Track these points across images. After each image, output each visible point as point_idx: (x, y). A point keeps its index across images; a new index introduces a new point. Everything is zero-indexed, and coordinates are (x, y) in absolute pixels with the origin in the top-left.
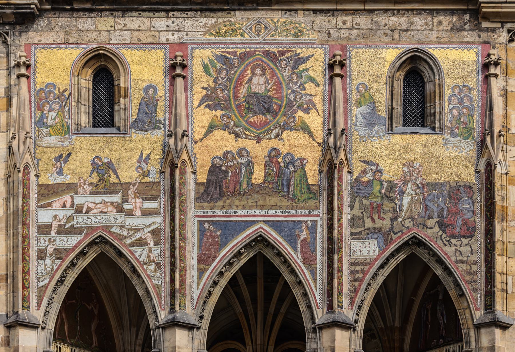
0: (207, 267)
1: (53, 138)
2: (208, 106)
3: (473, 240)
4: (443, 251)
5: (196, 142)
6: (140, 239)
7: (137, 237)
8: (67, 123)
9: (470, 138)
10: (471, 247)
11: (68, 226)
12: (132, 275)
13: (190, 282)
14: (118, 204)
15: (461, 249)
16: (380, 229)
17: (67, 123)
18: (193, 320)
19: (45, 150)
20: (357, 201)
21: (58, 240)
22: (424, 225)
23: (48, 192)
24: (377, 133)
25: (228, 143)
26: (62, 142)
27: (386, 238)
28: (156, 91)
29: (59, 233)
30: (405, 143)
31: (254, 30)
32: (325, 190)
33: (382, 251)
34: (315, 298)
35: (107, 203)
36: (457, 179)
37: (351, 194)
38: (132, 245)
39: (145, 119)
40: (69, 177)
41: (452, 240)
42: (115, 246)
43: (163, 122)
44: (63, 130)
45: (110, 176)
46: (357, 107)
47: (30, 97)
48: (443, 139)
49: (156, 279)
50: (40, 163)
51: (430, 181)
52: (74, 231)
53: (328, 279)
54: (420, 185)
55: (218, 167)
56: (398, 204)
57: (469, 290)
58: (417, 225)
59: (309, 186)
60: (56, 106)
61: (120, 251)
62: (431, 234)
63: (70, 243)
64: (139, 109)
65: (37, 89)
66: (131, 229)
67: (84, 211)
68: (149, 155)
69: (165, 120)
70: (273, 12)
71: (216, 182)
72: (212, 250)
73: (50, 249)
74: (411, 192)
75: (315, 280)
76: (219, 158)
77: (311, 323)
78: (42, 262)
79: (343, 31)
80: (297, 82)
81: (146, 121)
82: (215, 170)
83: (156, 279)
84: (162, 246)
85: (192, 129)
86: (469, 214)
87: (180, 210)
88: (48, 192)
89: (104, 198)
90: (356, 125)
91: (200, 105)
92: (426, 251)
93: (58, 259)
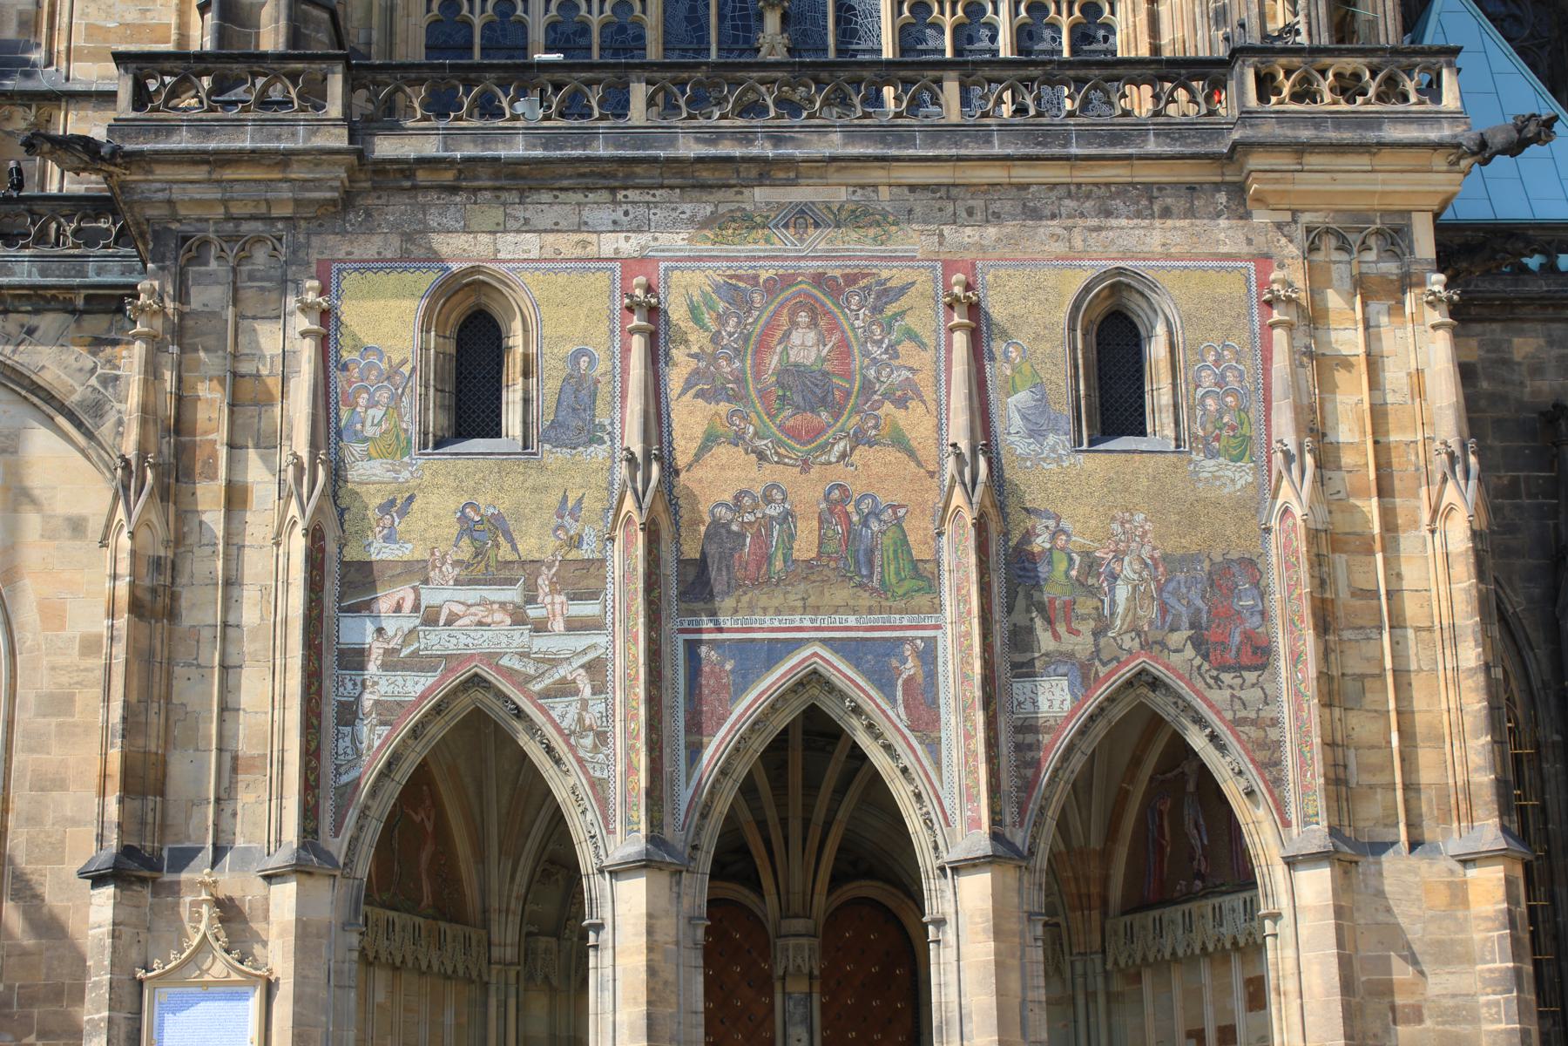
1: (376, 463)
2: (700, 394)
6: (563, 681)
7: (557, 677)
15: (1242, 694)
20: (1021, 595)
21: (383, 682)
22: (1163, 644)
24: (1053, 449)
25: (743, 475)
26: (395, 471)
27: (1084, 676)
35: (492, 603)
38: (546, 694)
39: (575, 423)
40: (410, 546)
41: (1223, 676)
43: (609, 428)
44: (395, 447)
45: (498, 547)
51: (1169, 551)
52: (419, 663)
57: (1265, 782)
59: (915, 564)
60: (383, 396)
61: (517, 707)
62: (1178, 662)
63: (410, 689)
66: (543, 661)
69: (612, 424)
75: (938, 764)
84: (610, 695)
91: (684, 392)
93: (383, 723)
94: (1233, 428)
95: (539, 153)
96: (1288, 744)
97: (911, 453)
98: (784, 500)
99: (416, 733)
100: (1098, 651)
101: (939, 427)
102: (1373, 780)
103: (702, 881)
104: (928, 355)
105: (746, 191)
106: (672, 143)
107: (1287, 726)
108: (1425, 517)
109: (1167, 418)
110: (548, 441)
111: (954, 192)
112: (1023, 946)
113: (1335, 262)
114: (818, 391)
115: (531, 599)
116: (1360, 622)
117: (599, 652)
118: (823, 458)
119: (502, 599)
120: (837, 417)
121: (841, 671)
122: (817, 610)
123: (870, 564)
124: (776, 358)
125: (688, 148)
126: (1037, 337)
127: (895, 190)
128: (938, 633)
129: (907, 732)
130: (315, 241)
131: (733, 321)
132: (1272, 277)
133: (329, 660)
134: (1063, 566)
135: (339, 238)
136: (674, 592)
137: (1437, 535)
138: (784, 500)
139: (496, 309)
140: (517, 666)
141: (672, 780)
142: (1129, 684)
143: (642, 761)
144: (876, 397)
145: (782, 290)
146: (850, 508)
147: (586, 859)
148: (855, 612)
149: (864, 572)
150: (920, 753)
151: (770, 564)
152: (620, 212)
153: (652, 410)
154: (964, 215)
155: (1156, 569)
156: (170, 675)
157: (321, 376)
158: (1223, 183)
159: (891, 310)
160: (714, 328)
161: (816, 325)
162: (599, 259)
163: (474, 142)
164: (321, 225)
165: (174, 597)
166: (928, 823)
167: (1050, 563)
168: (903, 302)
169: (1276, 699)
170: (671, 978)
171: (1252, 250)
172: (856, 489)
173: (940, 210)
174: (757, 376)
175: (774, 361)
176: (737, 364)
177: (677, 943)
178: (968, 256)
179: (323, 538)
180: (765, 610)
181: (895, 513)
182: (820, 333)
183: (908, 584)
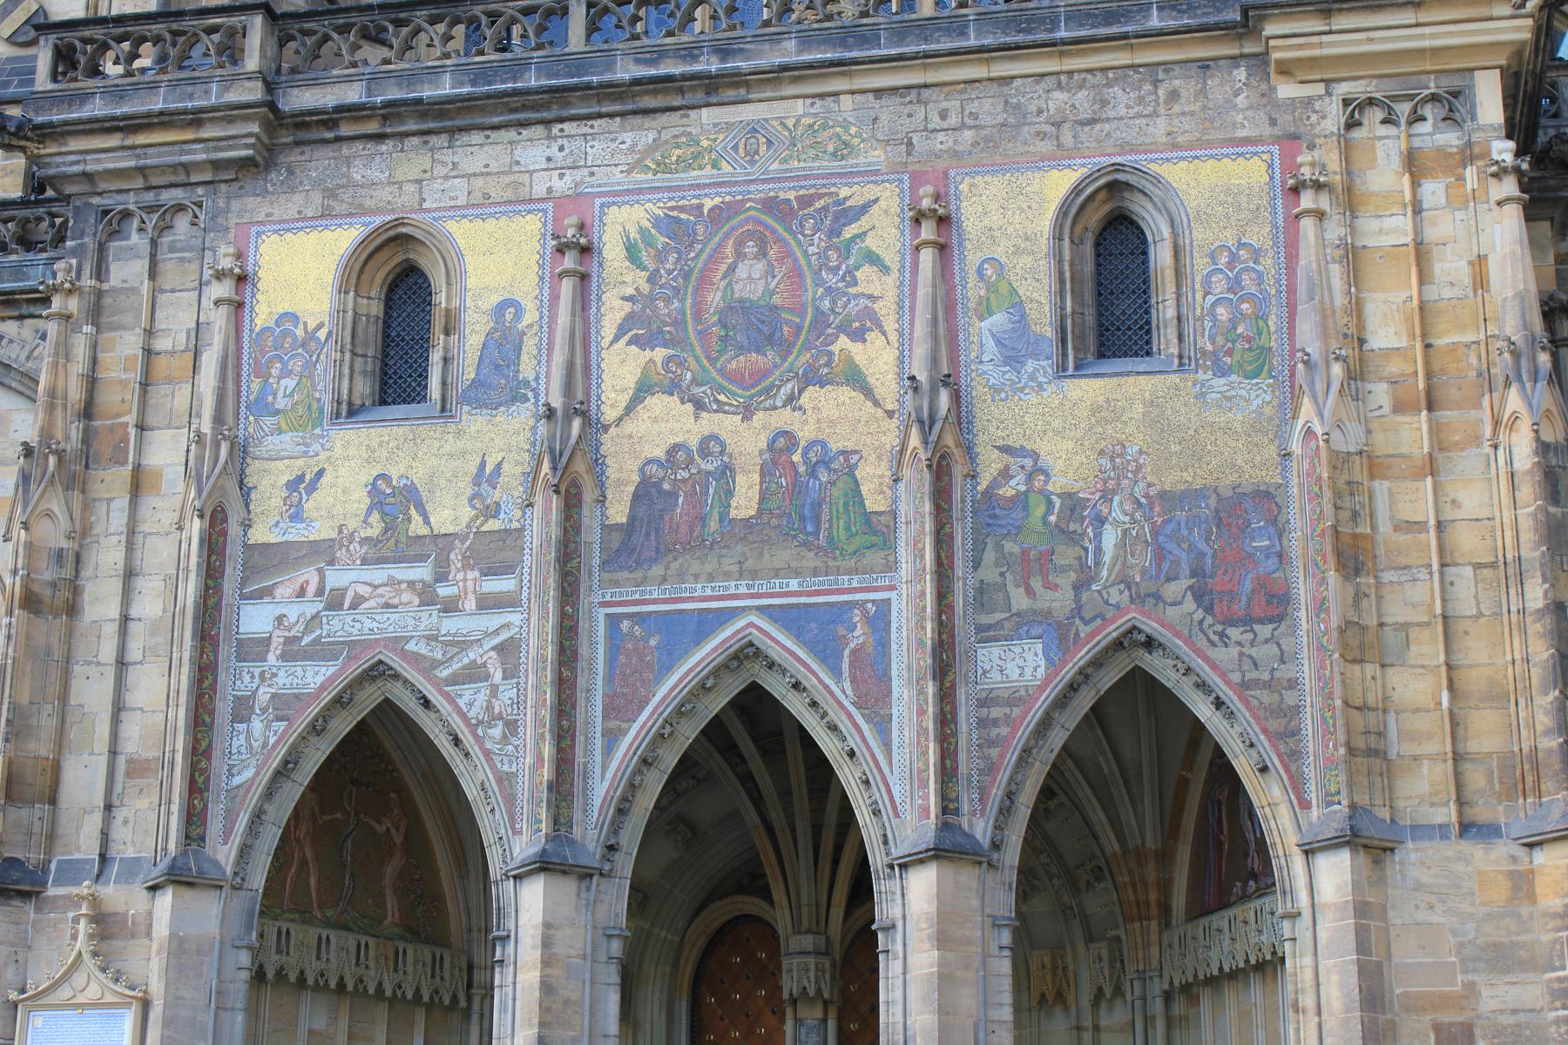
0: (625, 726)
1: (286, 437)
3: (1283, 627)
5: (606, 428)
7: (466, 661)
8: (319, 400)
9: (1264, 374)
10: (1279, 645)
11: (306, 640)
15: (1253, 652)
16: (1049, 612)
17: (319, 400)
19: (267, 465)
20: (990, 546)
21: (282, 673)
22: (1157, 597)
24: (1032, 377)
25: (679, 425)
27: (1061, 636)
28: (519, 311)
29: (285, 656)
30: (1101, 400)
34: (889, 791)
35: (400, 582)
36: (1234, 478)
38: (454, 680)
40: (317, 524)
41: (1229, 631)
43: (534, 384)
44: (307, 419)
45: (409, 520)
47: (239, 348)
48: (1195, 383)
50: (253, 496)
52: (320, 651)
53: (919, 742)
54: (1143, 500)
57: (1279, 755)
58: (1138, 599)
59: (868, 517)
60: (297, 365)
61: (424, 697)
63: (309, 680)
65: (257, 329)
67: (346, 606)
68: (499, 466)
69: (537, 379)
73: (264, 695)
75: (887, 746)
78: (242, 727)
81: (498, 385)
82: (646, 492)
83: (506, 759)
86: (1270, 562)
89: (394, 573)
90: (981, 362)
91: (616, 339)
92: (1171, 662)
93: (279, 719)
94: (1249, 340)
95: (466, 90)
96: (1308, 709)
97: (868, 392)
98: (722, 453)
99: (316, 728)
100: (1079, 608)
101: (901, 360)
102: (1418, 750)
104: (891, 280)
105: (692, 113)
106: (610, 67)
107: (1307, 687)
109: (1171, 333)
111: (926, 93)
113: (1380, 138)
115: (441, 577)
116: (1404, 561)
117: (513, 632)
118: (769, 403)
119: (412, 578)
121: (780, 642)
122: (754, 574)
124: (719, 294)
125: (627, 71)
126: (1017, 251)
127: (858, 97)
128: (893, 595)
129: (852, 709)
130: (235, 205)
131: (672, 257)
132: (1299, 160)
133: (226, 652)
134: (1040, 511)
135: (259, 199)
136: (596, 562)
137: (1500, 451)
138: (722, 453)
139: (424, 263)
140: (423, 651)
141: (585, 773)
142: (1118, 645)
143: (548, 750)
144: (830, 331)
145: (728, 220)
146: (796, 458)
147: (495, 868)
148: (797, 573)
149: (810, 528)
150: (867, 733)
151: (704, 525)
153: (579, 361)
154: (937, 119)
155: (1151, 509)
156: (66, 675)
157: (232, 347)
158: (1242, 56)
159: (848, 233)
160: (652, 267)
161: (765, 255)
162: (531, 201)
163: (399, 85)
164: (241, 188)
165: (76, 591)
166: (876, 813)
167: (1025, 508)
169: (1295, 657)
171: (1277, 131)
172: (805, 434)
173: (910, 115)
174: (698, 315)
175: (714, 299)
178: (940, 165)
179: (225, 520)
180: (696, 577)
181: (847, 460)
182: (769, 264)
183: (858, 541)
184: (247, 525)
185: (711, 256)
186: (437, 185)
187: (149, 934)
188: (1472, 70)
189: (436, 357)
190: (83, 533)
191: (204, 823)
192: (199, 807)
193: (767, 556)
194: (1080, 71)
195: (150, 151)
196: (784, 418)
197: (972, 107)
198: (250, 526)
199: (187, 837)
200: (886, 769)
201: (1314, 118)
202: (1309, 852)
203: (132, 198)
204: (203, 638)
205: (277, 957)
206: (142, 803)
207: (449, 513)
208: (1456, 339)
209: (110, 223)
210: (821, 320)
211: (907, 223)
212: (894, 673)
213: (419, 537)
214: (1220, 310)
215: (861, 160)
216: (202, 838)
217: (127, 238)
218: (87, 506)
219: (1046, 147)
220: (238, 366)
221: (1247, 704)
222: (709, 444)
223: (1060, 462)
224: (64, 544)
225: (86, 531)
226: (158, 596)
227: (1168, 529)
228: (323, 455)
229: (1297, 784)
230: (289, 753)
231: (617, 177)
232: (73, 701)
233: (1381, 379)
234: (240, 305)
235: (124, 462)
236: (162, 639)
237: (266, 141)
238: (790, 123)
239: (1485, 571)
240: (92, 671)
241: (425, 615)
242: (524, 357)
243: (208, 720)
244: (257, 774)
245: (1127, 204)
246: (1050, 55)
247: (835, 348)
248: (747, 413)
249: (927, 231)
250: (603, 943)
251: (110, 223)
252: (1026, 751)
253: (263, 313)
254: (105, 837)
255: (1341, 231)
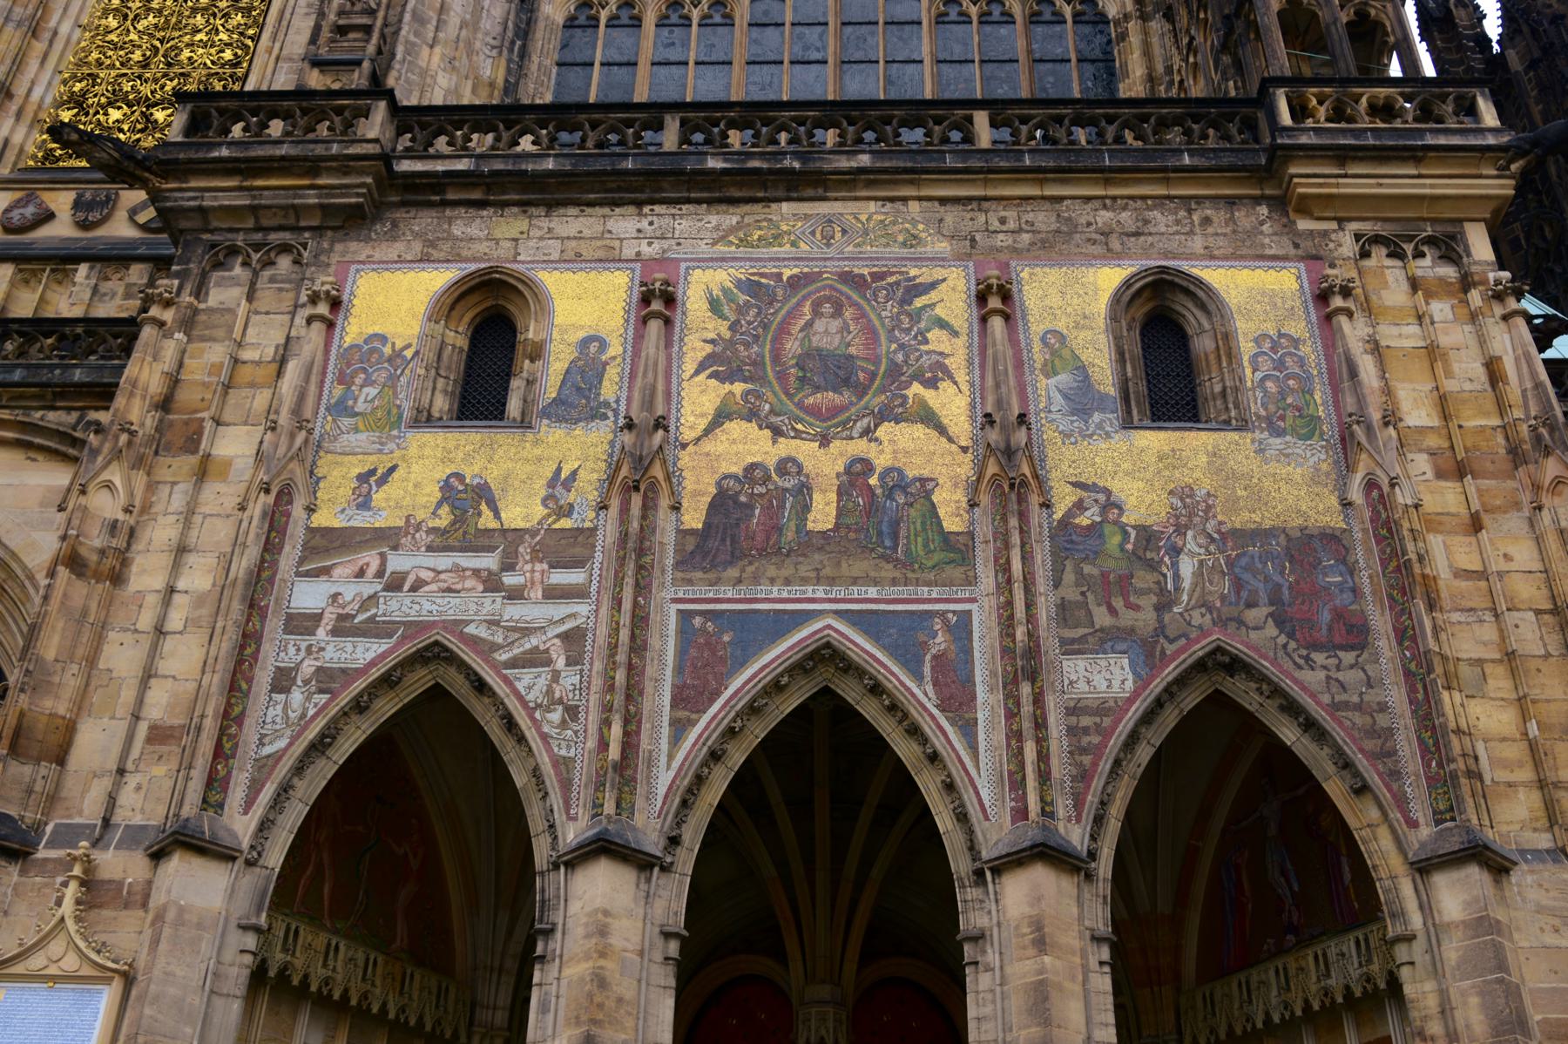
0: (694, 716)
1: (363, 436)
4: (1296, 681)
5: (684, 446)
7: (528, 646)
9: (1316, 437)
12: (504, 738)
13: (650, 752)
14: (490, 572)
18: (652, 842)
19: (339, 458)
21: (330, 648)
22: (1241, 623)
23: (327, 545)
24: (1100, 426)
26: (382, 444)
27: (1148, 652)
29: (335, 632)
31: (818, 236)
32: (986, 542)
33: (1142, 684)
35: (464, 570)
37: (1053, 554)
38: (514, 663)
40: (384, 514)
42: (469, 667)
44: (388, 422)
45: (480, 514)
46: (1047, 376)
48: (1253, 441)
49: (564, 744)
50: (321, 485)
52: (374, 629)
53: (1008, 745)
55: (730, 497)
56: (1169, 575)
57: (1380, 774)
58: (1222, 622)
59: (947, 539)
62: (1258, 638)
64: (563, 382)
66: (514, 629)
67: (406, 588)
68: (574, 473)
69: (617, 401)
70: (858, 204)
71: (725, 529)
72: (710, 677)
73: (308, 668)
74: (1197, 550)
75: (973, 748)
76: (734, 477)
77: (969, 860)
79: (1001, 236)
80: (909, 330)
81: (577, 401)
82: (723, 503)
83: (564, 744)
84: (587, 667)
85: (678, 419)
87: (637, 584)
88: (327, 545)
91: (697, 373)
93: (321, 691)
97: (942, 430)
98: (799, 473)
99: (359, 706)
101: (972, 406)
102: (1512, 778)
103: (681, 882)
104: (961, 342)
105: (774, 206)
108: (1526, 498)
110: (549, 418)
111: (986, 205)
112: (1086, 970)
114: (841, 373)
115: (508, 567)
120: (860, 398)
121: (860, 645)
122: (832, 581)
123: (895, 536)
126: (1077, 326)
127: (925, 203)
128: (973, 607)
129: (935, 711)
130: (339, 247)
133: (274, 626)
134: (1117, 539)
136: (669, 562)
137: (1545, 512)
145: (805, 286)
146: (873, 481)
147: (542, 853)
148: (876, 583)
149: (888, 543)
152: (644, 224)
159: (919, 302)
166: (962, 817)
167: (1101, 536)
168: (933, 296)
170: (629, 994)
171: (1300, 252)
172: (881, 461)
174: (776, 358)
175: (792, 347)
176: (756, 348)
177: (641, 953)
178: (1003, 257)
179: (290, 502)
180: (772, 581)
183: (936, 557)
184: (311, 510)
185: (789, 314)
186: (532, 243)
187: (144, 905)
188: (1461, 221)
189: (516, 384)
190: (140, 510)
191: (225, 790)
192: (222, 773)
193: (844, 565)
194: (1122, 197)
195: (266, 193)
196: (859, 447)
197: (1030, 217)
198: (313, 511)
199: (204, 801)
200: (973, 772)
201: (1332, 245)
202: (1423, 868)
203: (241, 236)
204: (251, 606)
205: (281, 956)
206: (160, 770)
207: (521, 510)
208: (1483, 422)
209: (216, 254)
210: (895, 372)
211: (973, 299)
212: (978, 679)
213: (487, 530)
214: (1269, 384)
215: (929, 248)
216: (221, 806)
217: (231, 269)
218: (151, 487)
219: (1098, 250)
220: (324, 373)
221: (1340, 724)
222: (784, 466)
223: (1133, 499)
224: (121, 516)
225: (146, 508)
226: (209, 572)
227: (1244, 561)
228: (397, 454)
229: (1402, 802)
230: (327, 726)
231: (703, 249)
232: (101, 666)
233: (1421, 451)
234: (331, 325)
235: (195, 451)
236: (205, 612)
237: (376, 195)
238: (863, 218)
239: (1546, 617)
240: (128, 638)
241: (488, 602)
242: (605, 383)
243: (244, 686)
244: (290, 744)
245: (1168, 303)
246: (1096, 182)
247: (910, 392)
248: (825, 441)
249: (994, 302)
250: (659, 942)
251: (216, 254)
252: (1117, 763)
253: (354, 330)
254: (112, 801)
255: (1370, 330)
